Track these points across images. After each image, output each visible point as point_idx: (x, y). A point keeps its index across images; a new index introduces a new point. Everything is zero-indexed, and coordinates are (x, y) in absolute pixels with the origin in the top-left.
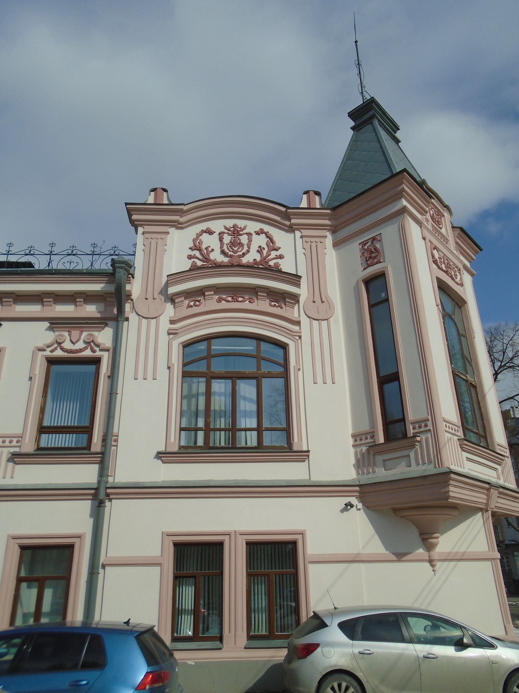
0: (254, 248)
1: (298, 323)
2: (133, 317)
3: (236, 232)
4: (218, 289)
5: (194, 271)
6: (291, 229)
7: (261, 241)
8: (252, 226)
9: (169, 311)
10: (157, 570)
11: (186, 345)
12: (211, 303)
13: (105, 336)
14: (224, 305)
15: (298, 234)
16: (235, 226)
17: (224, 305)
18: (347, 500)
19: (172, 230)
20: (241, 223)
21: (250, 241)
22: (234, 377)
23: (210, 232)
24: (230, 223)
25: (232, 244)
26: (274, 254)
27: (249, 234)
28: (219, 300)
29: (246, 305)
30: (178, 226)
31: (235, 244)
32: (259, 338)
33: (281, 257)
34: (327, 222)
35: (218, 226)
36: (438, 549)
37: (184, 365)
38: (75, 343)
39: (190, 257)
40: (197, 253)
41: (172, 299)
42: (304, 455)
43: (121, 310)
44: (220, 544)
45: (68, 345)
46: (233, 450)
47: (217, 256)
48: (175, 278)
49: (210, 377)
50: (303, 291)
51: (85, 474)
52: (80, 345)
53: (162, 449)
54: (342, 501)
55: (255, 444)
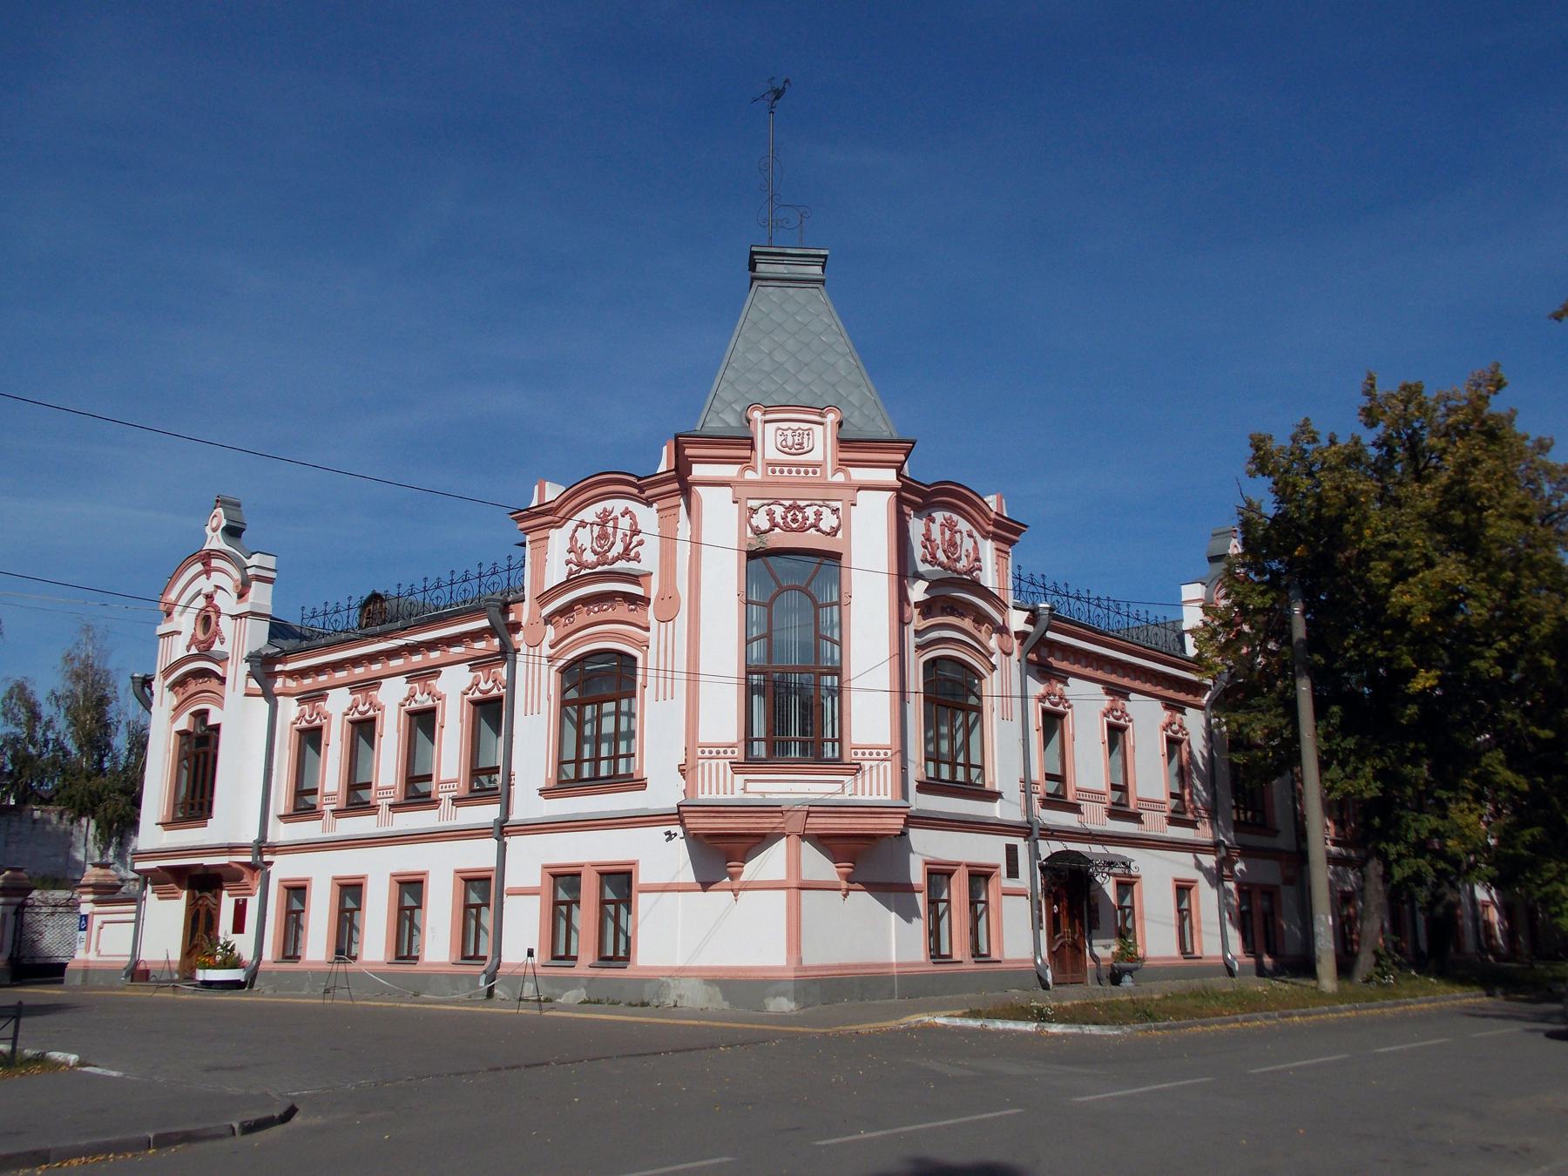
0: (620, 534)
1: (647, 629)
2: (524, 648)
5: (570, 583)
6: (649, 504)
7: (625, 523)
8: (618, 505)
9: (550, 630)
10: (538, 898)
11: (563, 671)
12: (581, 617)
13: (503, 672)
16: (605, 510)
17: (593, 617)
18: (667, 829)
19: (553, 533)
21: (615, 528)
22: (600, 701)
23: (583, 524)
24: (598, 507)
26: (636, 539)
27: (616, 518)
29: (610, 614)
30: (557, 525)
31: (603, 536)
33: (640, 543)
34: (676, 486)
35: (589, 514)
36: (743, 878)
37: (564, 692)
38: (488, 686)
39: (568, 562)
41: (548, 620)
42: (641, 784)
45: (483, 686)
46: (596, 784)
47: (589, 557)
48: (544, 598)
49: (581, 704)
51: (487, 813)
52: (490, 684)
53: (543, 785)
54: (659, 832)
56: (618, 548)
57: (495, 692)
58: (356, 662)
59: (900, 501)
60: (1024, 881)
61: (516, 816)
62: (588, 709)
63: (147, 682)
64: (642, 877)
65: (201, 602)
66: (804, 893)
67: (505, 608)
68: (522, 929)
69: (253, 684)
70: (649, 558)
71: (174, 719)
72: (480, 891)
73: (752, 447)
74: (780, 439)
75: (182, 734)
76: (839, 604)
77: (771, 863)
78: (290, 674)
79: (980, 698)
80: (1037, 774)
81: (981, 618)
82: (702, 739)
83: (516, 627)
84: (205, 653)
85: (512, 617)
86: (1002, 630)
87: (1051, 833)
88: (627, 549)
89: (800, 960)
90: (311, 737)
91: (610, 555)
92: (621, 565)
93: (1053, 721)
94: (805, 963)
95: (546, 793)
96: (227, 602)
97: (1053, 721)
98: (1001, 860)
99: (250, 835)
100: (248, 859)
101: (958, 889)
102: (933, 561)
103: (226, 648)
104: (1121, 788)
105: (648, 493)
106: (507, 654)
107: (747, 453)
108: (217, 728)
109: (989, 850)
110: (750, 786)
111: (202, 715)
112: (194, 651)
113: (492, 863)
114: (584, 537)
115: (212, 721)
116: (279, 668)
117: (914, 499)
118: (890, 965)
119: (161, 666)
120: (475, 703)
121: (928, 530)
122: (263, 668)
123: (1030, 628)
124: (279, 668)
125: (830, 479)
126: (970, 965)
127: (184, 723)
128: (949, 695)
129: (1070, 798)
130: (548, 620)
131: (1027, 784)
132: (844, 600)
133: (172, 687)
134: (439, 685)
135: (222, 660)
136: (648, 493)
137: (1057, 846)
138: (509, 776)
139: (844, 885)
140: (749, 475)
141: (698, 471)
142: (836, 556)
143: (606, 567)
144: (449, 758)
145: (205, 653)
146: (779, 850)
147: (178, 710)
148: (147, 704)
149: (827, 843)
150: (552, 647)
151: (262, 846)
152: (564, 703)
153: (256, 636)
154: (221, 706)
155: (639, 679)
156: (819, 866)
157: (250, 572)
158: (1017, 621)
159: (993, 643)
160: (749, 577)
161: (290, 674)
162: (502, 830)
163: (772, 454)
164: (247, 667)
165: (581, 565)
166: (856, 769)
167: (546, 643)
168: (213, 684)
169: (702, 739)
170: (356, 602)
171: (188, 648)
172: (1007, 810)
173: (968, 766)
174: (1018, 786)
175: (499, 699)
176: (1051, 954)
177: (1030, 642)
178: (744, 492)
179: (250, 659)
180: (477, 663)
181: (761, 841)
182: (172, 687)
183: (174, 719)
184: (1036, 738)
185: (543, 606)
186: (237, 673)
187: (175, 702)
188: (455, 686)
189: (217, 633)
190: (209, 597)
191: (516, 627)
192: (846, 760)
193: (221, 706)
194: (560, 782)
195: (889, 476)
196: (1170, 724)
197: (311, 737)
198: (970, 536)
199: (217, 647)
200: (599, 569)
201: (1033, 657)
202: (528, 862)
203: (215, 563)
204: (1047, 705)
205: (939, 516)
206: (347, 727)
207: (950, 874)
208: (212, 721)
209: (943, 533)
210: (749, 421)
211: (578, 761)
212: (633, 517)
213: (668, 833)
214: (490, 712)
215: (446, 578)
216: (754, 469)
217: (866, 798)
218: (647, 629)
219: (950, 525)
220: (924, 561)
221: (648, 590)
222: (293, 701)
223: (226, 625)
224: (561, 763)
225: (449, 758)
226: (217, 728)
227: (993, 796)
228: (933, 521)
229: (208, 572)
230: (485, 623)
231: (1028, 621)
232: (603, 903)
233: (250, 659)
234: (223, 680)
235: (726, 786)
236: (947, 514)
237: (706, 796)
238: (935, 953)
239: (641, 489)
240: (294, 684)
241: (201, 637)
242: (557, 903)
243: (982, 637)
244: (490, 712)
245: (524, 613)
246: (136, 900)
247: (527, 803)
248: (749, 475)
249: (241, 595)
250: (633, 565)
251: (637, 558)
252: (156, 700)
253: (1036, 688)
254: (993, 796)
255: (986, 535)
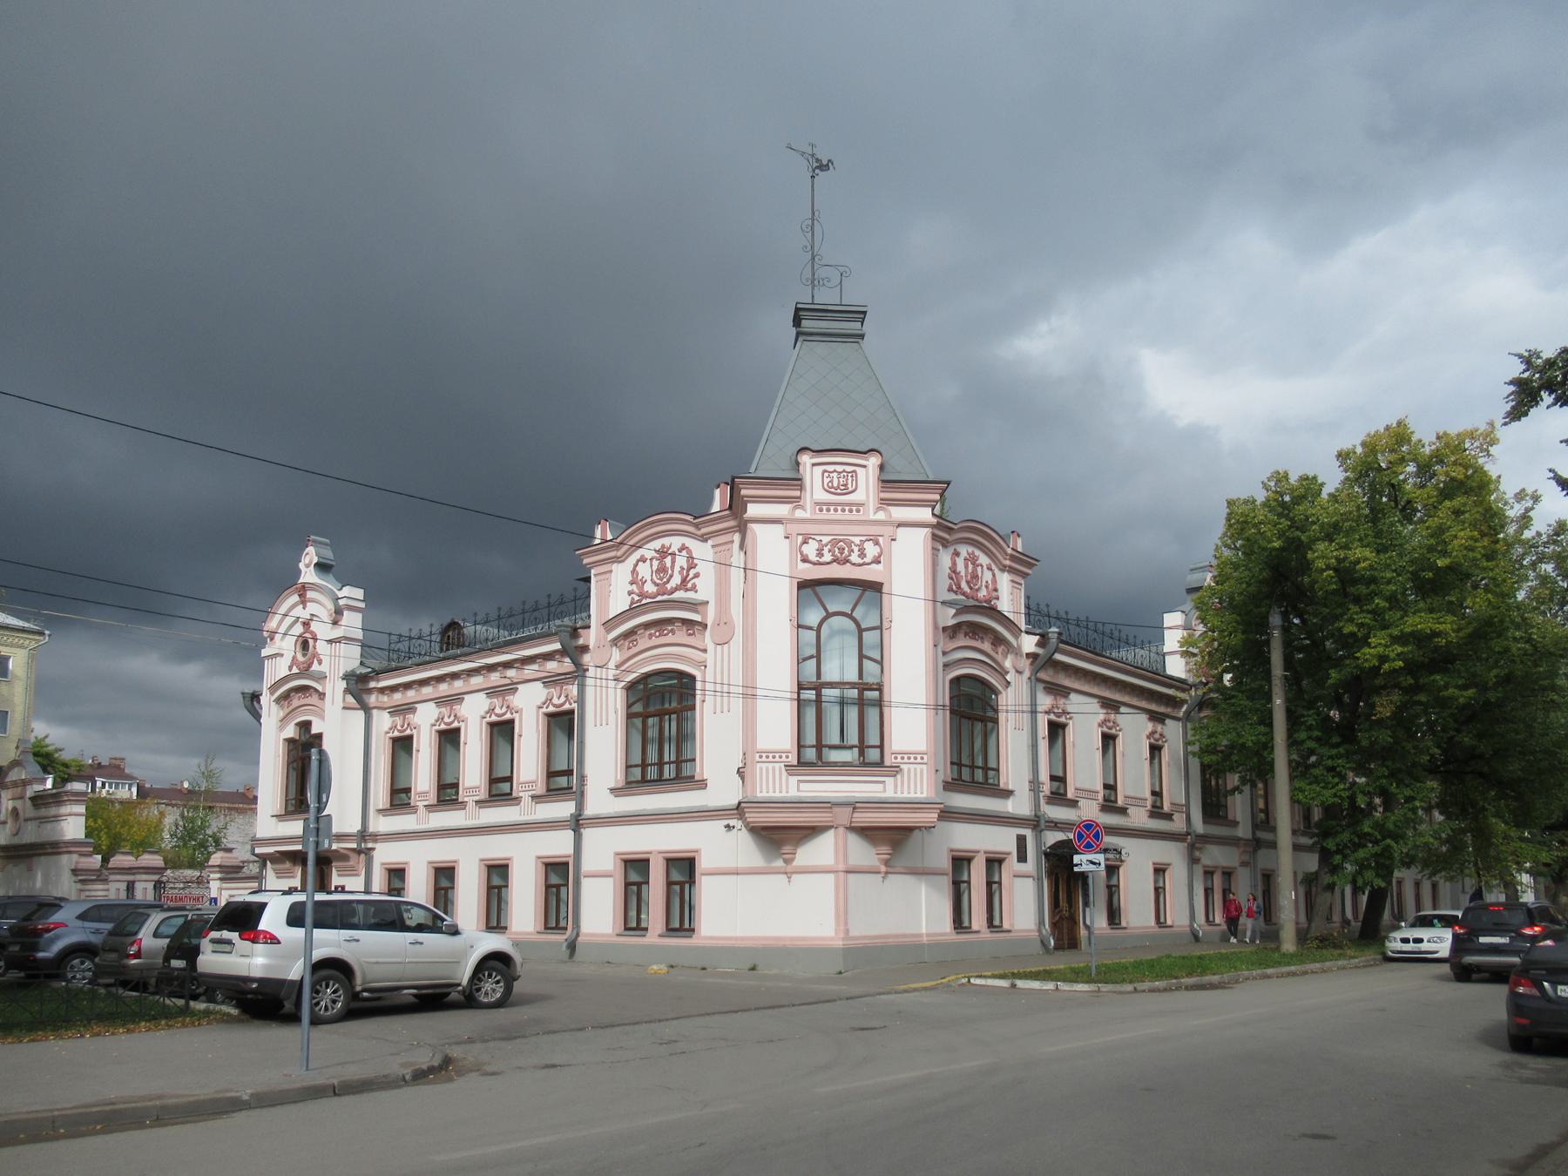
0: (677, 569)
1: (705, 651)
3: (663, 553)
4: (647, 626)
6: (704, 539)
7: (681, 561)
8: (675, 542)
9: (616, 656)
12: (643, 642)
13: (573, 690)
14: (655, 641)
15: (710, 542)
17: (655, 641)
20: (666, 541)
21: (673, 562)
22: (660, 714)
24: (657, 544)
25: (658, 571)
26: (692, 572)
27: (673, 554)
28: (651, 636)
29: (670, 639)
30: (619, 560)
31: (662, 569)
32: (681, 674)
33: (697, 576)
35: (648, 551)
37: (629, 706)
39: (630, 593)
40: (634, 587)
42: (702, 784)
43: (577, 663)
44: (648, 860)
45: (555, 701)
47: (650, 588)
48: (609, 624)
49: (645, 717)
50: (711, 616)
53: (612, 785)
55: (673, 775)
56: (676, 580)
57: (567, 707)
58: (440, 679)
59: (935, 537)
60: (1030, 866)
61: (590, 810)
62: (650, 721)
63: (255, 697)
64: (703, 864)
65: (298, 629)
66: (851, 876)
67: (575, 633)
68: (598, 910)
69: (351, 700)
70: (705, 589)
71: (281, 728)
72: (559, 879)
73: (801, 488)
74: (826, 481)
75: (290, 741)
76: (880, 628)
77: (821, 850)
78: (382, 690)
79: (996, 711)
80: (1044, 776)
81: (998, 640)
82: (762, 744)
83: (585, 649)
84: (305, 671)
85: (581, 642)
86: (1017, 651)
87: (1056, 825)
88: (684, 581)
89: (847, 931)
90: (403, 745)
91: (669, 586)
92: (679, 595)
93: (1056, 730)
94: (853, 933)
95: (615, 791)
96: (323, 630)
97: (1056, 730)
98: (1012, 847)
99: (354, 826)
100: (354, 846)
101: (977, 874)
102: (959, 590)
103: (324, 668)
104: (1110, 787)
105: (704, 530)
106: (579, 673)
107: (797, 493)
108: (319, 736)
109: (1002, 840)
110: (803, 786)
111: (306, 726)
112: (295, 670)
113: (570, 850)
114: (645, 571)
115: (314, 730)
116: (372, 684)
117: (944, 533)
118: (921, 935)
119: (268, 681)
120: (550, 716)
121: (954, 564)
122: (358, 685)
123: (1040, 651)
124: (372, 684)
125: (872, 517)
126: (986, 935)
127: (291, 731)
128: (969, 708)
129: (1070, 795)
130: (615, 642)
131: (1035, 785)
132: (885, 625)
133: (278, 701)
134: (517, 700)
135: (321, 677)
136: (704, 530)
137: (1060, 836)
138: (582, 778)
139: (883, 868)
140: (799, 514)
141: (753, 510)
142: (875, 587)
143: (665, 597)
144: (529, 762)
145: (305, 671)
146: (829, 836)
147: (283, 721)
148: (257, 716)
149: (868, 833)
150: (617, 667)
151: (363, 835)
152: (630, 716)
153: (350, 658)
154: (322, 718)
155: (698, 698)
156: (863, 853)
157: (341, 602)
158: (1029, 643)
159: (1008, 664)
160: (800, 605)
161: (382, 690)
162: (577, 823)
163: (822, 496)
164: (344, 684)
165: (643, 595)
166: (895, 771)
167: (612, 665)
168: (314, 699)
169: (762, 744)
170: (436, 628)
171: (290, 668)
172: (1020, 805)
173: (986, 769)
174: (1027, 786)
175: (572, 712)
176: (1054, 925)
177: (1040, 662)
178: (794, 529)
179: (347, 677)
180: (550, 681)
181: (810, 832)
182: (278, 701)
183: (281, 728)
184: (1043, 745)
185: (609, 631)
186: (335, 689)
187: (282, 714)
188: (530, 704)
189: (315, 655)
190: (306, 624)
191: (585, 649)
192: (887, 763)
193: (322, 718)
194: (628, 783)
195: (925, 514)
196: (1153, 733)
197: (403, 745)
198: (989, 568)
199: (315, 667)
200: (659, 598)
201: (1042, 675)
202: (602, 852)
203: (310, 594)
204: (1052, 717)
205: (964, 550)
206: (435, 737)
207: (969, 860)
208: (314, 730)
209: (966, 567)
210: (798, 464)
211: (644, 765)
212: (689, 552)
213: (728, 826)
214: (563, 724)
215: (544, 602)
216: (802, 508)
217: (900, 796)
218: (705, 651)
219: (972, 559)
220: (950, 590)
221: (705, 615)
222: (385, 715)
223: (322, 647)
224: (628, 767)
225: (529, 762)
226: (319, 736)
227: (1007, 794)
228: (957, 554)
229: (304, 602)
230: (557, 646)
231: (1039, 644)
232: (670, 884)
233: (347, 677)
234: (322, 695)
235: (780, 785)
236: (971, 549)
237: (764, 794)
238: (959, 923)
239: (697, 526)
240: (385, 698)
241: (300, 658)
242: (627, 885)
243: (999, 657)
244: (563, 724)
245: (592, 637)
246: (259, 878)
247: (599, 800)
248: (799, 514)
249: (335, 623)
250: (690, 595)
251: (694, 588)
252: (264, 713)
253: (1045, 701)
254: (1007, 794)
255: (1003, 569)
